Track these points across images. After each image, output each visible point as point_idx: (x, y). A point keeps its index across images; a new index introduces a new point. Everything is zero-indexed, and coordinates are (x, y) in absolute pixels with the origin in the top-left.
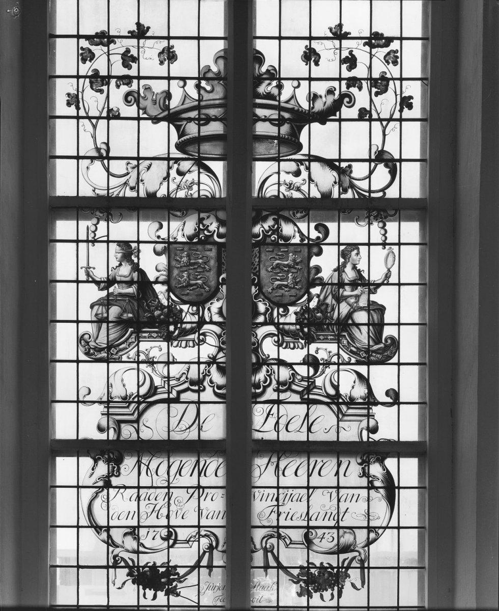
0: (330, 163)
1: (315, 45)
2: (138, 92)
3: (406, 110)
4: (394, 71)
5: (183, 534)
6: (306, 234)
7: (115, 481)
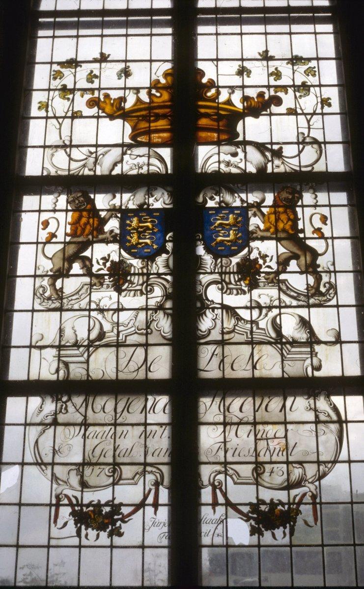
0: (261, 147)
1: (247, 64)
2: (99, 98)
3: (326, 107)
4: (312, 80)
5: (127, 471)
6: (245, 199)
7: (61, 418)
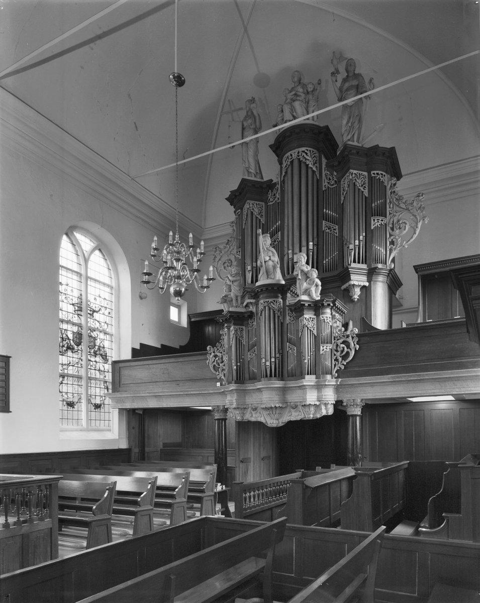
1: (96, 297)
5: (75, 395)
